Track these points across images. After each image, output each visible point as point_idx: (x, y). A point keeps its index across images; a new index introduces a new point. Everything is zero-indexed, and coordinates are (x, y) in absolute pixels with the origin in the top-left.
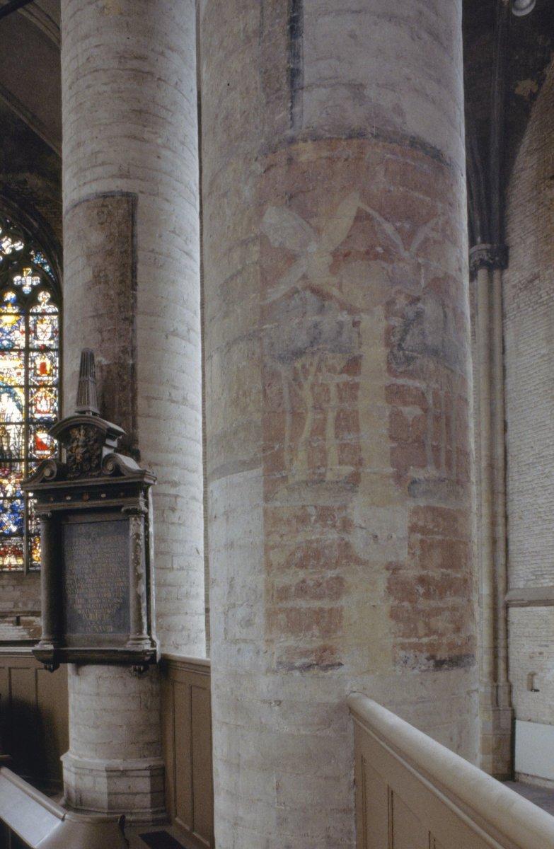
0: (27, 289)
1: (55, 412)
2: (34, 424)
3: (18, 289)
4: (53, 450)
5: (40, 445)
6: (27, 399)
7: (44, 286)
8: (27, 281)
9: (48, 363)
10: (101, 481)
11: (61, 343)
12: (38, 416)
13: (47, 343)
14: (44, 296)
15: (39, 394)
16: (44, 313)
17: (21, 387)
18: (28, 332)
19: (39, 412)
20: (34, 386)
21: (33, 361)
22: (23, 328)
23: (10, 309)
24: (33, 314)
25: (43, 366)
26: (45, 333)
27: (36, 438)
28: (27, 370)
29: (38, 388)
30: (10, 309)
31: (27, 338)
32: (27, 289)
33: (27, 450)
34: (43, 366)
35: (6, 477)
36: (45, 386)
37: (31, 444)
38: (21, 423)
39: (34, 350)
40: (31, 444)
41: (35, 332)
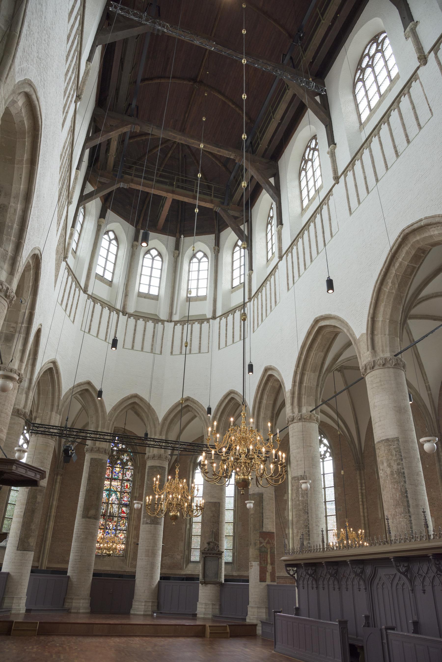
0: (125, 460)
1: (129, 501)
2: (122, 505)
3: (122, 460)
4: (127, 514)
5: (123, 512)
6: (120, 496)
7: (131, 460)
8: (125, 458)
9: (129, 485)
10: (216, 552)
11: (133, 478)
12: (123, 502)
13: (129, 478)
14: (129, 463)
15: (125, 495)
16: (129, 469)
17: (119, 492)
18: (123, 474)
19: (124, 501)
20: (123, 492)
21: (124, 484)
22: (122, 472)
23: (118, 466)
24: (126, 468)
25: (127, 485)
26: (129, 475)
27: (122, 509)
28: (122, 486)
29: (125, 493)
30: (118, 466)
31: (123, 476)
32: (125, 460)
33: (119, 513)
34: (127, 485)
35: (110, 522)
36: (127, 492)
37: (120, 511)
38: (118, 504)
39: (125, 480)
40: (120, 511)
41: (126, 474)
